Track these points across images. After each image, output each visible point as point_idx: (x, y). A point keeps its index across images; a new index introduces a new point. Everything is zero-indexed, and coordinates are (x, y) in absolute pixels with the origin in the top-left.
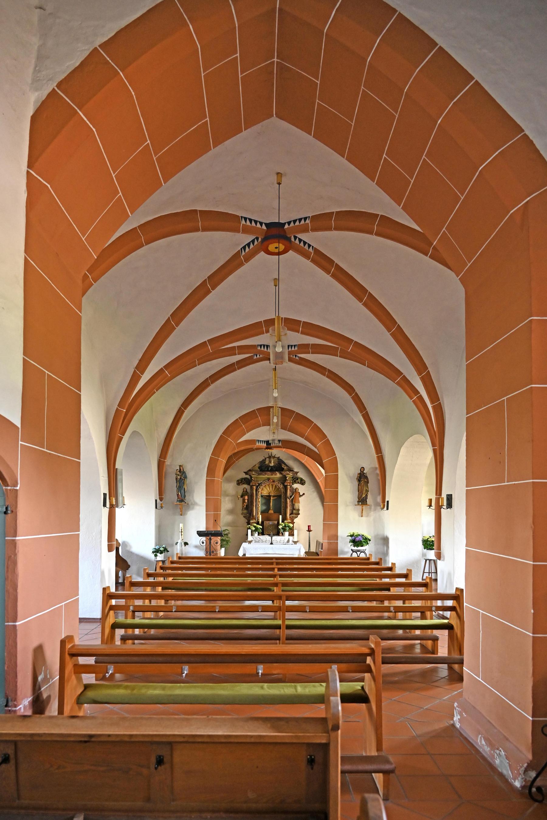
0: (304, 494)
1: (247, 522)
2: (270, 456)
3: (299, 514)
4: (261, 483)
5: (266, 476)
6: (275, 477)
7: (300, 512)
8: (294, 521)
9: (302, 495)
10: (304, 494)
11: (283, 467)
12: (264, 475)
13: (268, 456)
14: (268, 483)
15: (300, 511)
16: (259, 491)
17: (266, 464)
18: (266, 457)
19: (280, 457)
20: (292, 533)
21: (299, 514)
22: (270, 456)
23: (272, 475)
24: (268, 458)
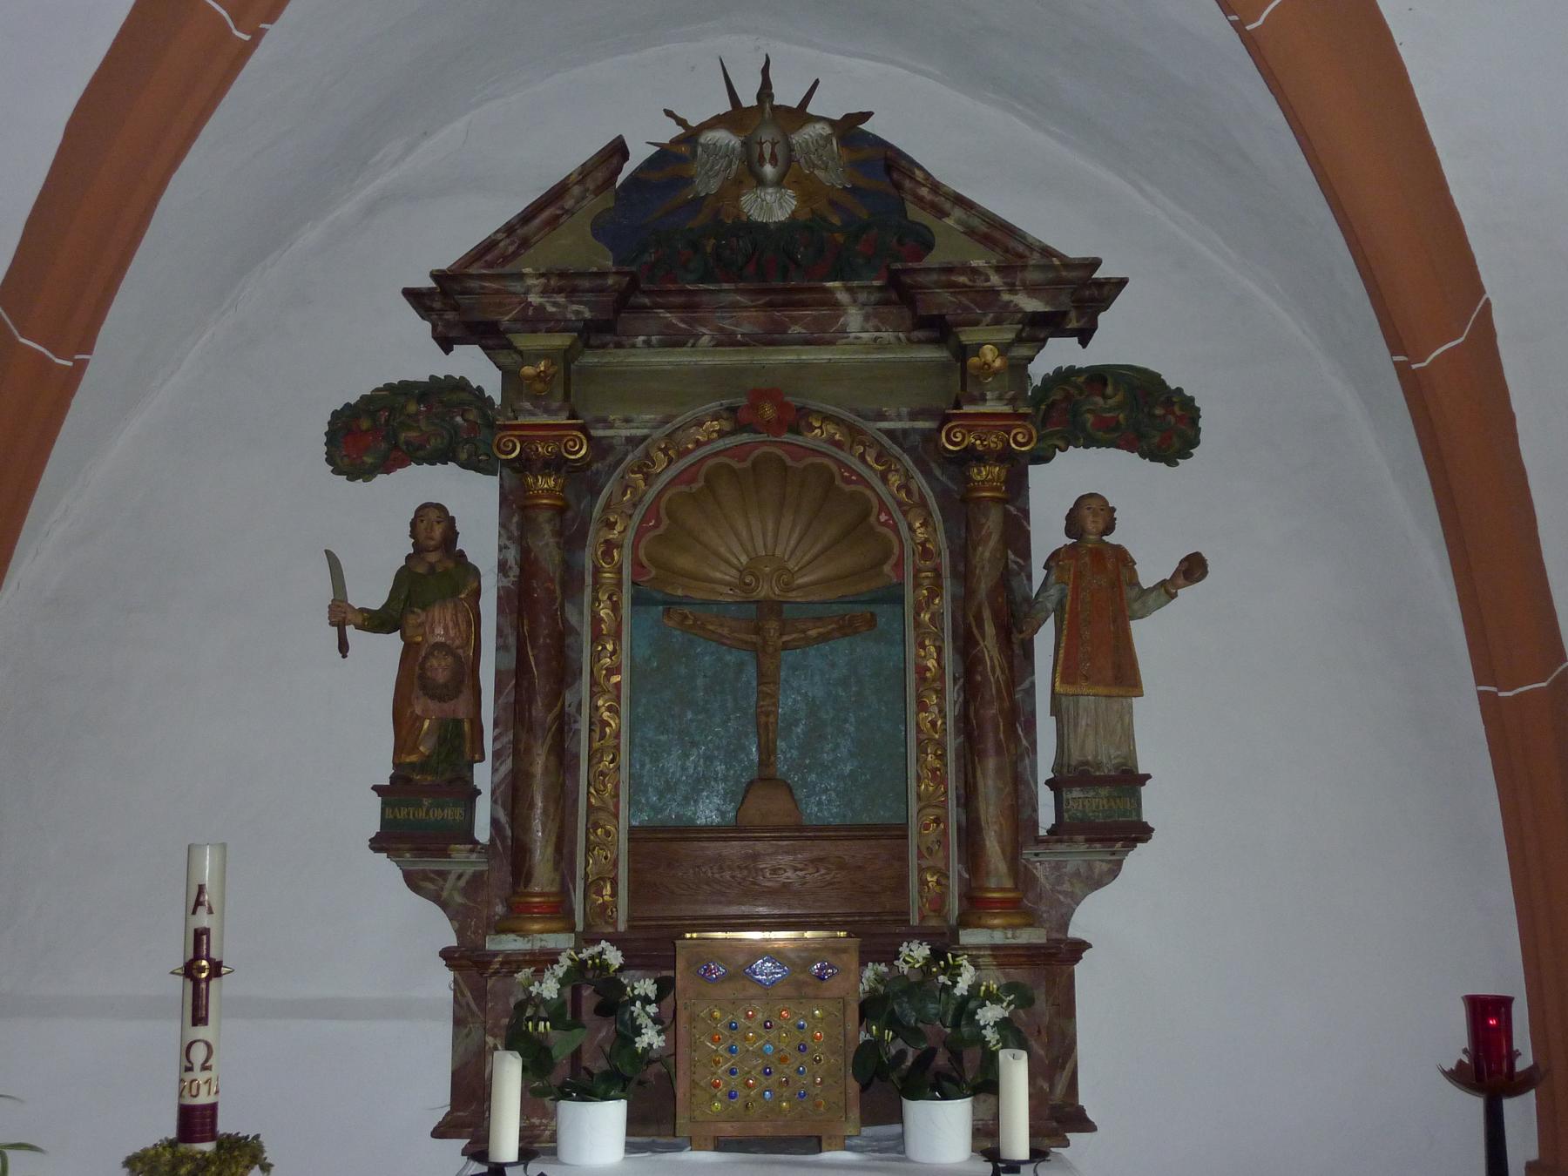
0: (1193, 568)
1: (447, 955)
2: (748, 99)
3: (1142, 833)
4: (633, 442)
5: (702, 357)
6: (802, 366)
7: (1153, 805)
8: (1074, 932)
9: (1167, 590)
10: (1193, 568)
11: (915, 214)
12: (674, 341)
13: (725, 106)
14: (721, 444)
15: (1146, 791)
16: (610, 546)
17: (698, 201)
18: (694, 122)
19: (866, 116)
20: (1060, 1089)
21: (1142, 833)
22: (748, 99)
23: (772, 337)
24: (717, 122)
